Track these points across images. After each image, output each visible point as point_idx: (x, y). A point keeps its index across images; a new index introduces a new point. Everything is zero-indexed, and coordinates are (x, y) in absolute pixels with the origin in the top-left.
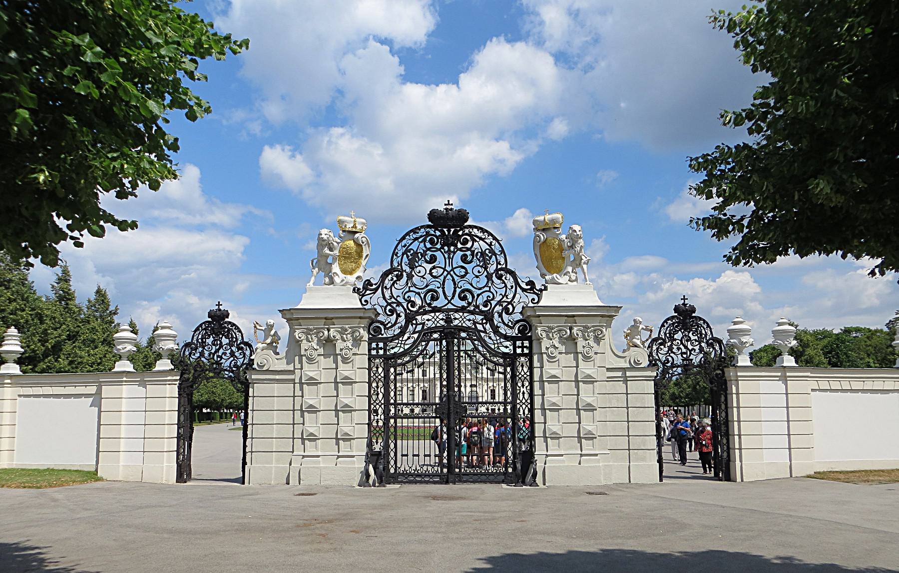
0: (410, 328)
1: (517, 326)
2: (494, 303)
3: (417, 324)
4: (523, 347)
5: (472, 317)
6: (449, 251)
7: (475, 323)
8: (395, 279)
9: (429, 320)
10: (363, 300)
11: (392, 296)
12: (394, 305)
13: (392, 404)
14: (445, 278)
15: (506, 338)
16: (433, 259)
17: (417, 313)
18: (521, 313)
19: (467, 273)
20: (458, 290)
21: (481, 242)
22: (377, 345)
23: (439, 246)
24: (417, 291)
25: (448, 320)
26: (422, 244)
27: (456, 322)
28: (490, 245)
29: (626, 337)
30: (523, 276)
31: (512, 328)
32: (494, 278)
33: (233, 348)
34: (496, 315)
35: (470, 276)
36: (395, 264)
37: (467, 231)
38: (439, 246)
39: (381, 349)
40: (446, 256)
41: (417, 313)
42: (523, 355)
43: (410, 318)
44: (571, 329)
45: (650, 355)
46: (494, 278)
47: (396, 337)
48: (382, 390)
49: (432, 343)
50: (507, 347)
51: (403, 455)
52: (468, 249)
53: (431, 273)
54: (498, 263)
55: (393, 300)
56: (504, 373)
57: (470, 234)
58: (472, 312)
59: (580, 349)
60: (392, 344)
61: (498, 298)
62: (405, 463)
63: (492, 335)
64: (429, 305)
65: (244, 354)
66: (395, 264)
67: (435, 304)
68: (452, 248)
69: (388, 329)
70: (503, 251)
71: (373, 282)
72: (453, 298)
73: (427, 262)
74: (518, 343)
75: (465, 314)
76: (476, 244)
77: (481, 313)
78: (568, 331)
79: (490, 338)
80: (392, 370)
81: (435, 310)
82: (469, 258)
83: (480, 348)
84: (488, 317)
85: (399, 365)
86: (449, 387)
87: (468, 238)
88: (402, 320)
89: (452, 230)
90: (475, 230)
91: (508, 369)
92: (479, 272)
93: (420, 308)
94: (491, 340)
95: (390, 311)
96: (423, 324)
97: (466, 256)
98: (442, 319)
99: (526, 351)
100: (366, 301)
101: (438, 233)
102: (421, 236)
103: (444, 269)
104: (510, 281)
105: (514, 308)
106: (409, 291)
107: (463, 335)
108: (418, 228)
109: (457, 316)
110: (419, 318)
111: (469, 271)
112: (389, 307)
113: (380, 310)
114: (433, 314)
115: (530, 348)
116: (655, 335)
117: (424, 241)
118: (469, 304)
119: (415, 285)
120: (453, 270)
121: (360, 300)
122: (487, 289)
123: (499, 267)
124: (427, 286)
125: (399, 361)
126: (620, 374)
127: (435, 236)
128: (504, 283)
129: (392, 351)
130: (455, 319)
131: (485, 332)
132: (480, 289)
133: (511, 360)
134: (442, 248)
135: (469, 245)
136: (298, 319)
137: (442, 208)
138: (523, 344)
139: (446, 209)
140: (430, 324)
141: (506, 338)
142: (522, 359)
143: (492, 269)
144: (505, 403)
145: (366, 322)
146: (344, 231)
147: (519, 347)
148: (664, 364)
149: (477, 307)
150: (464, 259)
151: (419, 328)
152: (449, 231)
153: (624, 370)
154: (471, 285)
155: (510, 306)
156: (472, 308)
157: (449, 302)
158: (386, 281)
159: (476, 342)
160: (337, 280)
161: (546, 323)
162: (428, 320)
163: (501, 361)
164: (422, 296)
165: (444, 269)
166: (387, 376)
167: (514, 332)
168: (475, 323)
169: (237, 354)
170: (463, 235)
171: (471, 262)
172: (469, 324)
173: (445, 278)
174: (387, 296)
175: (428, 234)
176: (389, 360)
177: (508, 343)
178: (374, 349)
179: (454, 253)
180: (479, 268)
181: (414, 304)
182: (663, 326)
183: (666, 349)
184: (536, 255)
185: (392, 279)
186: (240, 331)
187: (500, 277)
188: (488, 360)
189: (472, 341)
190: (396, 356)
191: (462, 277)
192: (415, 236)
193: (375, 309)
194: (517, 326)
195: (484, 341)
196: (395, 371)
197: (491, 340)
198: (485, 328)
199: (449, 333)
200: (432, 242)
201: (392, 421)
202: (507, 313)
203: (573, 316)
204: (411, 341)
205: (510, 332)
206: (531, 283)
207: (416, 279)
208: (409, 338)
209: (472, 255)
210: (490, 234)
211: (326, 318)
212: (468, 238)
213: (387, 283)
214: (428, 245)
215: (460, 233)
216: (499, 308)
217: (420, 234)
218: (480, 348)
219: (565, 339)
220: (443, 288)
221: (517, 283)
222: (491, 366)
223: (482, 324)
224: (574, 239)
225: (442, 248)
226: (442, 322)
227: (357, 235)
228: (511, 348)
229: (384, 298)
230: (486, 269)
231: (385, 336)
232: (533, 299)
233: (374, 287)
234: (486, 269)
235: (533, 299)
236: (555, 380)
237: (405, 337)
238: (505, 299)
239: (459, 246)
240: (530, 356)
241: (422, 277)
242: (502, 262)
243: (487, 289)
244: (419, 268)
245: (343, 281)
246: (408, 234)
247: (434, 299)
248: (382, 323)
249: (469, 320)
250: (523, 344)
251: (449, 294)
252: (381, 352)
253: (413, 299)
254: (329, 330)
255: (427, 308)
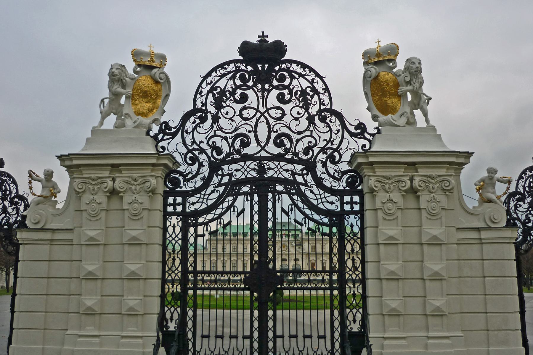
0: (215, 180)
1: (345, 177)
2: (316, 150)
3: (223, 175)
4: (352, 203)
5: (289, 167)
6: (263, 90)
7: (293, 174)
8: (198, 121)
9: (239, 171)
10: (160, 144)
11: (194, 142)
12: (197, 153)
13: (191, 272)
14: (258, 120)
15: (333, 192)
16: (244, 98)
17: (224, 162)
18: (350, 163)
19: (284, 114)
20: (273, 135)
21: (301, 79)
22: (175, 200)
23: (250, 83)
24: (224, 135)
25: (261, 170)
26: (231, 82)
27: (270, 173)
28: (312, 82)
29: (478, 191)
30: (351, 121)
31: (338, 180)
32: (317, 121)
33: (7, 203)
34: (319, 166)
35: (287, 119)
36: (199, 104)
37: (284, 66)
38: (250, 83)
39: (179, 204)
40: (260, 94)
41: (224, 162)
42: (352, 212)
43: (215, 167)
44: (412, 179)
45: (508, 212)
46: (317, 121)
47: (197, 191)
48: (180, 256)
49: (240, 198)
50: (332, 203)
51: (203, 336)
52: (285, 87)
53: (241, 115)
54: (322, 103)
55: (195, 146)
56: (330, 235)
57: (288, 70)
58: (291, 161)
59: (423, 204)
60: (192, 200)
61: (322, 144)
62: (205, 346)
63: (315, 188)
64: (238, 152)
65: (18, 210)
66: (199, 104)
67: (246, 151)
68: (266, 86)
69: (188, 180)
70: (327, 90)
71: (171, 124)
72: (267, 144)
73: (236, 101)
74: (347, 198)
75: (282, 164)
76: (295, 82)
77: (301, 162)
78: (409, 182)
79: (312, 192)
80: (192, 230)
81: (246, 158)
82: (287, 97)
83: (300, 204)
84: (310, 166)
85: (201, 224)
86: (263, 252)
87: (286, 74)
88: (205, 171)
89: (266, 66)
90: (294, 65)
91: (335, 230)
92: (298, 113)
93: (227, 155)
94: (313, 194)
95: (190, 158)
96: (231, 175)
97: (283, 95)
98: (254, 169)
99: (357, 207)
100: (163, 148)
101: (250, 68)
102: (230, 72)
103: (257, 110)
104: (336, 124)
105: (341, 156)
106: (215, 136)
107: (280, 188)
108: (228, 63)
109: (272, 165)
110: (225, 167)
111: (287, 112)
112: (190, 155)
113: (179, 159)
114: (242, 163)
115: (362, 203)
116: (512, 189)
117: (233, 78)
118: (287, 151)
119: (221, 129)
120: (267, 110)
121: (156, 146)
122: (309, 133)
123: (323, 107)
124: (236, 129)
125: (201, 220)
126: (474, 235)
127: (247, 71)
128: (328, 126)
129: (193, 208)
130: (270, 169)
131: (306, 184)
132: (300, 133)
133: (337, 218)
134: (255, 85)
135: (287, 83)
136: (79, 166)
137: (254, 40)
138: (352, 199)
139: (258, 41)
140: (238, 175)
141: (333, 192)
142: (352, 216)
143: (314, 110)
144: (331, 272)
145: (160, 172)
146: (139, 66)
147: (347, 203)
148: (524, 224)
149: (296, 154)
150: (281, 98)
151: (226, 179)
152: (263, 67)
153: (478, 230)
154: (289, 128)
155: (336, 154)
156: (290, 156)
157: (263, 148)
158: (188, 124)
159: (295, 197)
160: (129, 123)
161: (380, 172)
162: (237, 170)
163: (326, 220)
164: (230, 141)
165: (257, 110)
166: (185, 239)
167: (342, 185)
168: (293, 174)
169: (10, 210)
170: (280, 70)
171: (289, 101)
172: (286, 175)
173: (258, 120)
174: (188, 141)
175: (238, 70)
176: (189, 219)
177: (333, 199)
178: (170, 205)
179: (269, 91)
180: (298, 109)
181: (219, 151)
182: (521, 177)
183: (526, 206)
184: (366, 94)
185: (194, 121)
186: (14, 182)
187: (323, 119)
188: (310, 219)
189: (290, 195)
190: (197, 213)
191: (278, 119)
192: (222, 72)
193: (174, 158)
194: (345, 177)
195: (305, 196)
196: (196, 231)
197: (313, 194)
198: (305, 180)
199: (262, 186)
200: (242, 78)
201: (191, 292)
202: (333, 162)
203: (414, 164)
204: (215, 195)
205: (336, 185)
206: (361, 127)
207: (223, 122)
208: (213, 192)
209: (291, 94)
210: (311, 70)
211: (113, 166)
212: (286, 74)
213: (189, 126)
214: (238, 82)
215: (277, 68)
216: (322, 157)
217: (229, 70)
218: (300, 204)
219: (405, 191)
220: (255, 132)
221: (344, 127)
222: (312, 225)
223: (302, 175)
224: (414, 70)
225: (255, 85)
226: (254, 173)
227: (154, 71)
228: (338, 204)
229: (184, 143)
230: (307, 110)
231: (184, 189)
232: (364, 146)
233: (173, 130)
234: (307, 110)
235: (364, 146)
236: (392, 242)
237: (209, 191)
238: (329, 145)
239: (275, 83)
240: (361, 214)
241: (231, 119)
242: (327, 101)
243: (309, 133)
244: (227, 109)
245: (135, 122)
246: (215, 69)
247: (245, 144)
248: (181, 174)
249: (287, 170)
250: (352, 199)
251: (263, 138)
252: (179, 209)
253: (218, 145)
254: (114, 180)
255: (236, 156)
